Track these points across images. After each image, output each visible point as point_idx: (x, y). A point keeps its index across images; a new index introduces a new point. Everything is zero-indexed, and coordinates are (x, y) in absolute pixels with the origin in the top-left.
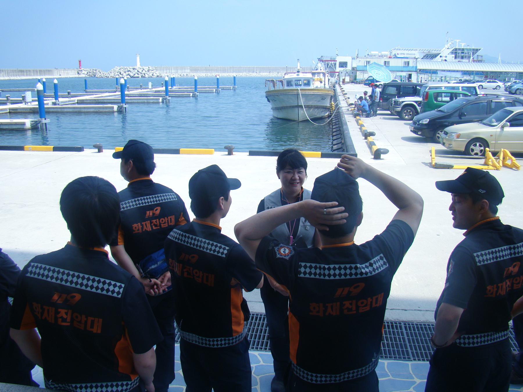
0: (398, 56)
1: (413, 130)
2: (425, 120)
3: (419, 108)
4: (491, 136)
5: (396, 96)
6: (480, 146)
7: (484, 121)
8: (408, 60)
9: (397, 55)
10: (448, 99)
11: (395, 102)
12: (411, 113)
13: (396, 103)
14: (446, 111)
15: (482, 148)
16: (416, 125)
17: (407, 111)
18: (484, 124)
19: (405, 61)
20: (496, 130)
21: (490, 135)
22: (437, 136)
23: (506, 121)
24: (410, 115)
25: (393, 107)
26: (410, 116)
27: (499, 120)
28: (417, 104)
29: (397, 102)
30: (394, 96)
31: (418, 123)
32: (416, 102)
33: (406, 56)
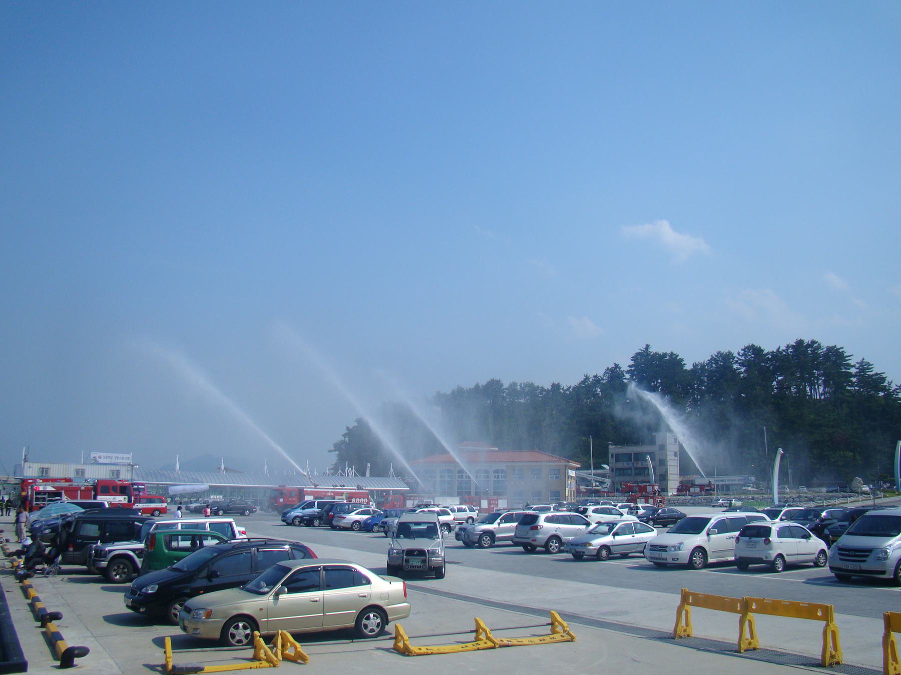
0: (101, 461)
1: (130, 604)
2: (152, 586)
3: (139, 562)
4: (261, 609)
5: (99, 541)
6: (245, 627)
7: (249, 586)
8: (118, 468)
9: (98, 459)
10: (187, 544)
11: (96, 551)
12: (126, 570)
13: (101, 554)
14: (186, 569)
15: (248, 631)
16: (137, 596)
17: (119, 567)
18: (249, 591)
19: (112, 469)
20: (268, 599)
21: (259, 609)
22: (173, 613)
23: (282, 585)
24: (125, 573)
25: (94, 560)
26: (124, 576)
27: (272, 583)
28: (135, 554)
29: (101, 551)
30: (95, 539)
31: (139, 593)
32: (133, 550)
33: (113, 461)
